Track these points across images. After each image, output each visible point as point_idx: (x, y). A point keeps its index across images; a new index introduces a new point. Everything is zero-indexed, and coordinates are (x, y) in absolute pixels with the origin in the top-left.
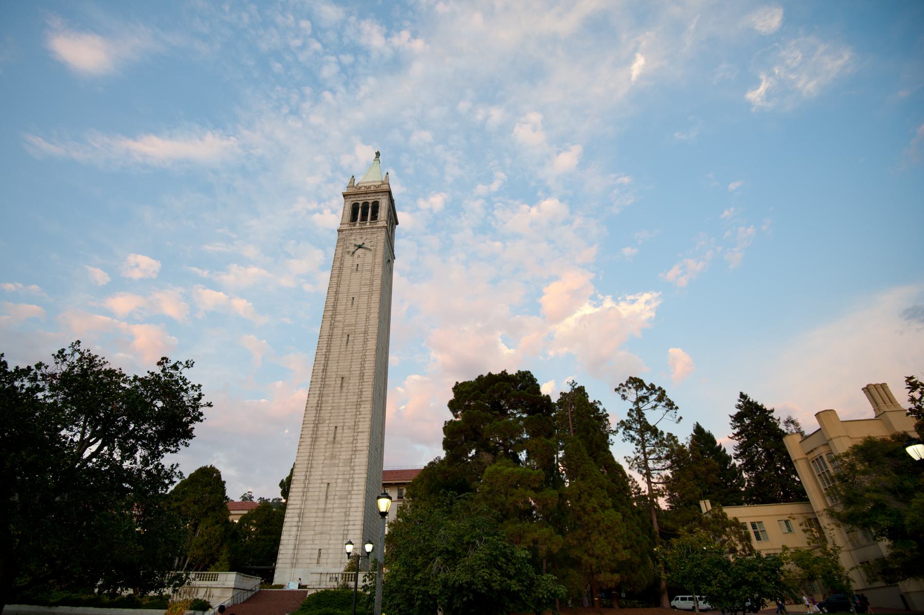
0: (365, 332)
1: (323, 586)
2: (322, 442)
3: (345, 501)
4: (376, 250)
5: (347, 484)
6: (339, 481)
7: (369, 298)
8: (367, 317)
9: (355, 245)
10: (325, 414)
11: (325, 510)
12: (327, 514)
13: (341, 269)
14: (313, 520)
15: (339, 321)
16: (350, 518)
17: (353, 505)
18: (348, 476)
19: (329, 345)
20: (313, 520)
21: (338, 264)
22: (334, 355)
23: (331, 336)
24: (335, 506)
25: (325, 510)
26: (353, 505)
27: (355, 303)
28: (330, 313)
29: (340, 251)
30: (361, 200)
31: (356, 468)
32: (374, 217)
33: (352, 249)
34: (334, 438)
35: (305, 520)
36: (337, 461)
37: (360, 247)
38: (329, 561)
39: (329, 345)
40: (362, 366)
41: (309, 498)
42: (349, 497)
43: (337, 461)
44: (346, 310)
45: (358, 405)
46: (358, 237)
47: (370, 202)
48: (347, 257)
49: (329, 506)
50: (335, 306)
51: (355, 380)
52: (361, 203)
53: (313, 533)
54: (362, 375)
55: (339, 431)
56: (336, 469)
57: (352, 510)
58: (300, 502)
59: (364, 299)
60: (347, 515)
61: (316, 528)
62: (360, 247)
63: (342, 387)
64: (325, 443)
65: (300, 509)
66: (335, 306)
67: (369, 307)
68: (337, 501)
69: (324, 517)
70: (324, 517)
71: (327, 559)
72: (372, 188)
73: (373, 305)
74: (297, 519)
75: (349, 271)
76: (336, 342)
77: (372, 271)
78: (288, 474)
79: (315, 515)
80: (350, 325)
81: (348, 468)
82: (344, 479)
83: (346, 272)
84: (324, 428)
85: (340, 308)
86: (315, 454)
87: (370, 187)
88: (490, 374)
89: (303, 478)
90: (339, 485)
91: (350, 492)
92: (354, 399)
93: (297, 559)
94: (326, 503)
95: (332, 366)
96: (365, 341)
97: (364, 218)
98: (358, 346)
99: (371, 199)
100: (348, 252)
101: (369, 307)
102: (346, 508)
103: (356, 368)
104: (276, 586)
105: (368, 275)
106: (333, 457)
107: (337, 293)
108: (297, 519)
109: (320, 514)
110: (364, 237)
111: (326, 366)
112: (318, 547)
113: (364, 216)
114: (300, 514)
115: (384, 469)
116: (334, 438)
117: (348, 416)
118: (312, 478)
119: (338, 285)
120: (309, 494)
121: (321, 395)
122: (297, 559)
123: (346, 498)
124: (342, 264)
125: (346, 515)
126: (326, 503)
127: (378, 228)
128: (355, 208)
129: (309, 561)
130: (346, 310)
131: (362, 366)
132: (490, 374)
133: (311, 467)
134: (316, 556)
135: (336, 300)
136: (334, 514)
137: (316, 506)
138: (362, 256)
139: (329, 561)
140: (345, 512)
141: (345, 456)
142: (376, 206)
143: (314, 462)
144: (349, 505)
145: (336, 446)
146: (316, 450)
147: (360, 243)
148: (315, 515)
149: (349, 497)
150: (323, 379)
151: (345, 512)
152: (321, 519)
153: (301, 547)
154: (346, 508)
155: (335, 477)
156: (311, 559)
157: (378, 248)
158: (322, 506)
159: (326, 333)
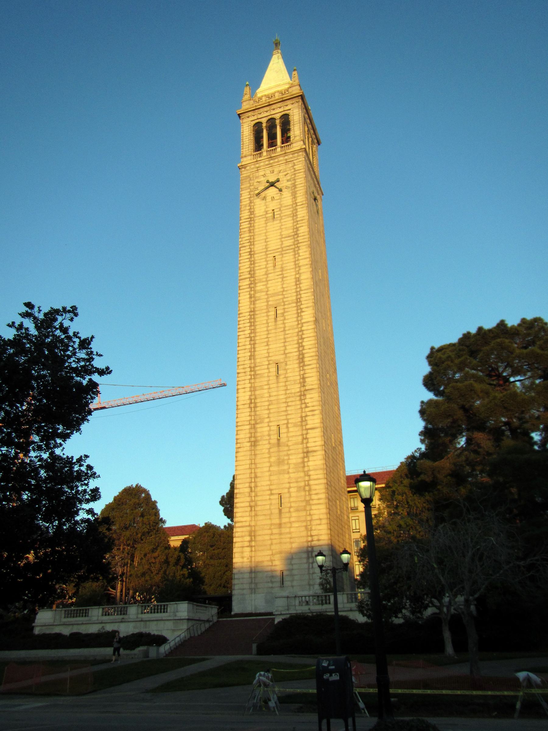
0: (298, 301)
1: (293, 611)
2: (263, 447)
3: (304, 513)
4: (294, 186)
5: (303, 493)
6: (291, 490)
7: (296, 252)
10: (262, 412)
11: (280, 525)
12: (284, 530)
14: (267, 537)
15: (261, 291)
16: (313, 533)
17: (315, 517)
18: (302, 484)
20: (267, 537)
24: (293, 519)
25: (280, 525)
26: (315, 517)
27: (278, 264)
30: (263, 117)
31: (311, 473)
32: (286, 139)
34: (278, 440)
35: (258, 538)
36: (286, 467)
38: (295, 583)
40: (300, 346)
41: (259, 513)
42: (308, 508)
43: (286, 467)
44: (267, 274)
45: (302, 395)
46: (268, 171)
47: (277, 116)
48: (258, 201)
49: (284, 520)
52: (264, 121)
53: (269, 552)
54: (301, 359)
56: (287, 476)
57: (314, 523)
58: (248, 519)
59: (289, 257)
61: (273, 547)
64: (268, 446)
65: (250, 526)
67: (297, 266)
68: (294, 514)
69: (280, 534)
71: (292, 581)
72: (277, 96)
73: (302, 263)
74: (248, 538)
75: (263, 221)
76: (261, 319)
77: (294, 215)
78: (227, 489)
79: (269, 532)
81: (302, 474)
82: (299, 488)
84: (263, 430)
85: (260, 273)
86: (257, 461)
87: (273, 95)
88: (480, 329)
89: (248, 490)
90: (293, 494)
91: (308, 502)
92: (296, 388)
93: (256, 584)
94: (280, 518)
95: (261, 351)
96: (299, 312)
99: (277, 113)
101: (297, 266)
102: (306, 521)
103: (292, 348)
104: (237, 615)
105: (288, 223)
106: (280, 462)
108: (248, 538)
109: (276, 531)
110: (276, 170)
114: (251, 532)
115: (348, 473)
116: (278, 440)
118: (258, 489)
120: (258, 508)
121: (253, 389)
122: (256, 584)
123: (305, 510)
124: (252, 212)
126: (280, 518)
127: (294, 152)
129: (270, 585)
131: (300, 346)
132: (480, 329)
133: (256, 477)
136: (292, 530)
137: (268, 522)
139: (295, 583)
140: (306, 527)
141: (295, 459)
142: (286, 121)
143: (258, 470)
144: (309, 518)
145: (282, 448)
146: (258, 457)
147: (272, 180)
148: (269, 532)
149: (308, 508)
151: (306, 527)
152: (277, 536)
154: (306, 521)
155: (287, 485)
156: (272, 582)
157: (298, 182)
158: (277, 521)
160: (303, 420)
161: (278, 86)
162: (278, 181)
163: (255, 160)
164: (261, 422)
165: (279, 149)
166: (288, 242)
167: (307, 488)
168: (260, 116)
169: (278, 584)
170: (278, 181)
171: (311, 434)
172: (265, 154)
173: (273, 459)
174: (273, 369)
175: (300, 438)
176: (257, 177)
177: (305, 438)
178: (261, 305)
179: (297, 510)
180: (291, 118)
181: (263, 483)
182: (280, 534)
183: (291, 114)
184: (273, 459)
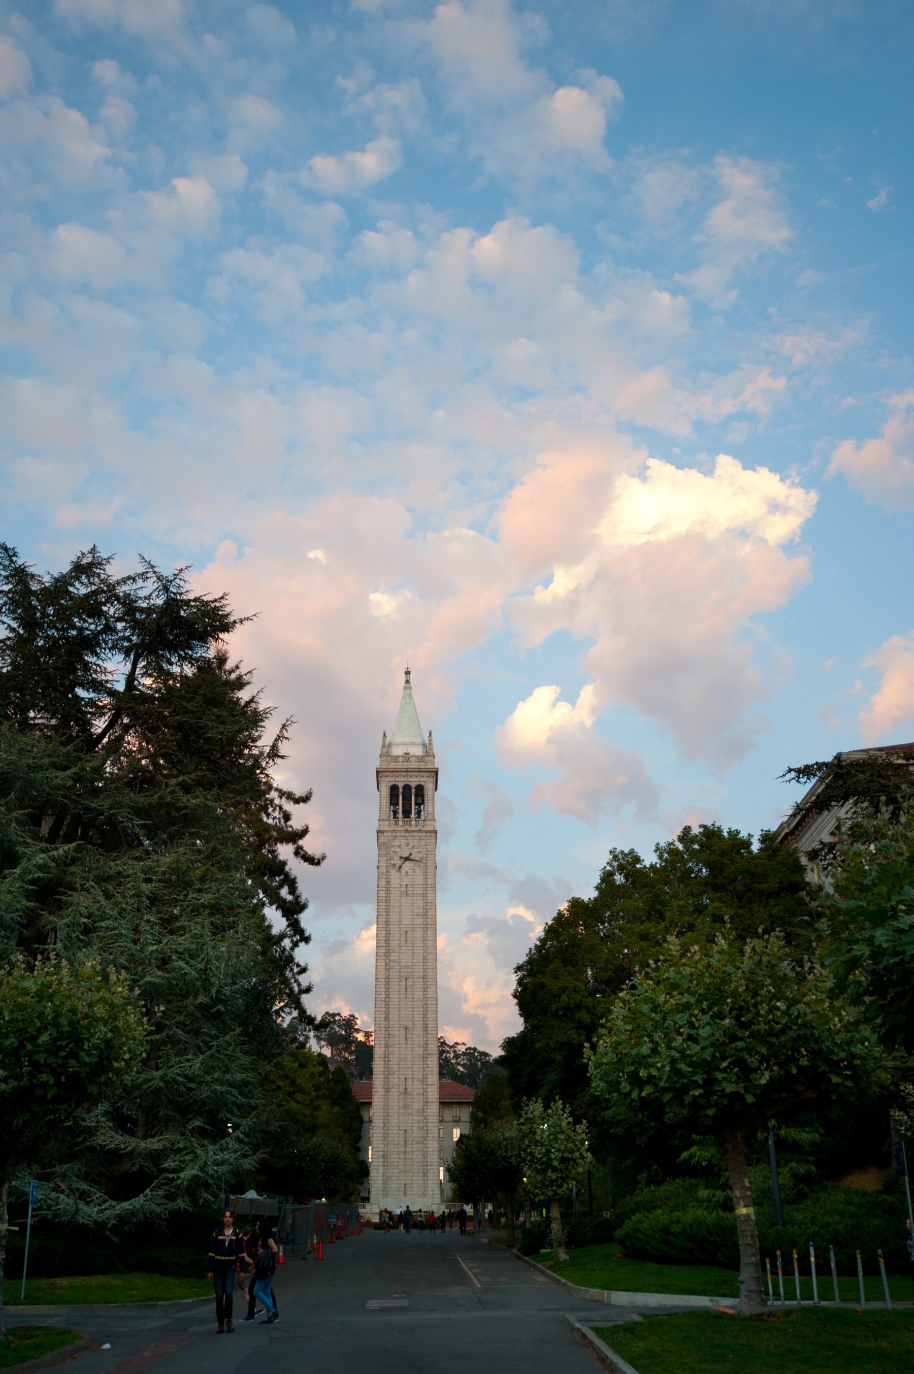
2: (394, 1093)
8: (425, 958)
9: (401, 858)
11: (405, 1153)
12: (408, 1156)
13: (387, 890)
15: (395, 961)
19: (387, 990)
21: (383, 883)
22: (394, 1001)
23: (388, 979)
28: (383, 950)
29: (383, 864)
33: (398, 862)
34: (406, 1089)
37: (407, 859)
39: (387, 990)
40: (425, 1016)
43: (410, 1111)
44: (400, 947)
45: (425, 1057)
48: (393, 872)
49: (408, 1149)
50: (387, 941)
51: (418, 1031)
52: (401, 785)
55: (409, 1082)
59: (419, 934)
60: (425, 1157)
62: (407, 859)
63: (406, 1039)
66: (387, 941)
68: (415, 1146)
70: (405, 1159)
72: (414, 765)
74: (382, 1160)
76: (395, 986)
80: (406, 967)
83: (395, 895)
85: (394, 944)
89: (382, 1125)
91: (425, 1138)
92: (420, 1051)
94: (405, 1147)
95: (394, 1015)
97: (407, 813)
98: (418, 994)
99: (413, 782)
100: (394, 865)
103: (418, 1017)
106: (406, 1107)
107: (387, 923)
108: (382, 1160)
109: (402, 1156)
111: (387, 1014)
112: (403, 1182)
113: (407, 799)
116: (406, 1089)
117: (416, 1068)
119: (388, 914)
121: (387, 1046)
124: (388, 883)
125: (424, 1158)
126: (405, 1147)
127: (427, 832)
128: (394, 789)
130: (400, 947)
134: (403, 1189)
135: (388, 933)
138: (410, 873)
141: (417, 1106)
147: (405, 855)
150: (387, 1028)
153: (389, 1182)
158: (402, 1149)
159: (382, 975)
160: (424, 1077)
161: (413, 744)
162: (411, 854)
163: (392, 828)
164: (393, 1074)
165: (413, 823)
166: (419, 921)
167: (425, 1129)
168: (398, 779)
169: (402, 1193)
170: (411, 854)
171: (430, 1089)
172: (401, 823)
173: (401, 1104)
174: (403, 1032)
175: (422, 1091)
176: (393, 846)
177: (425, 1091)
178: (394, 973)
179: (418, 1143)
180: (425, 791)
181: (394, 1121)
182: (405, 1159)
183: (426, 787)
184: (401, 1104)
